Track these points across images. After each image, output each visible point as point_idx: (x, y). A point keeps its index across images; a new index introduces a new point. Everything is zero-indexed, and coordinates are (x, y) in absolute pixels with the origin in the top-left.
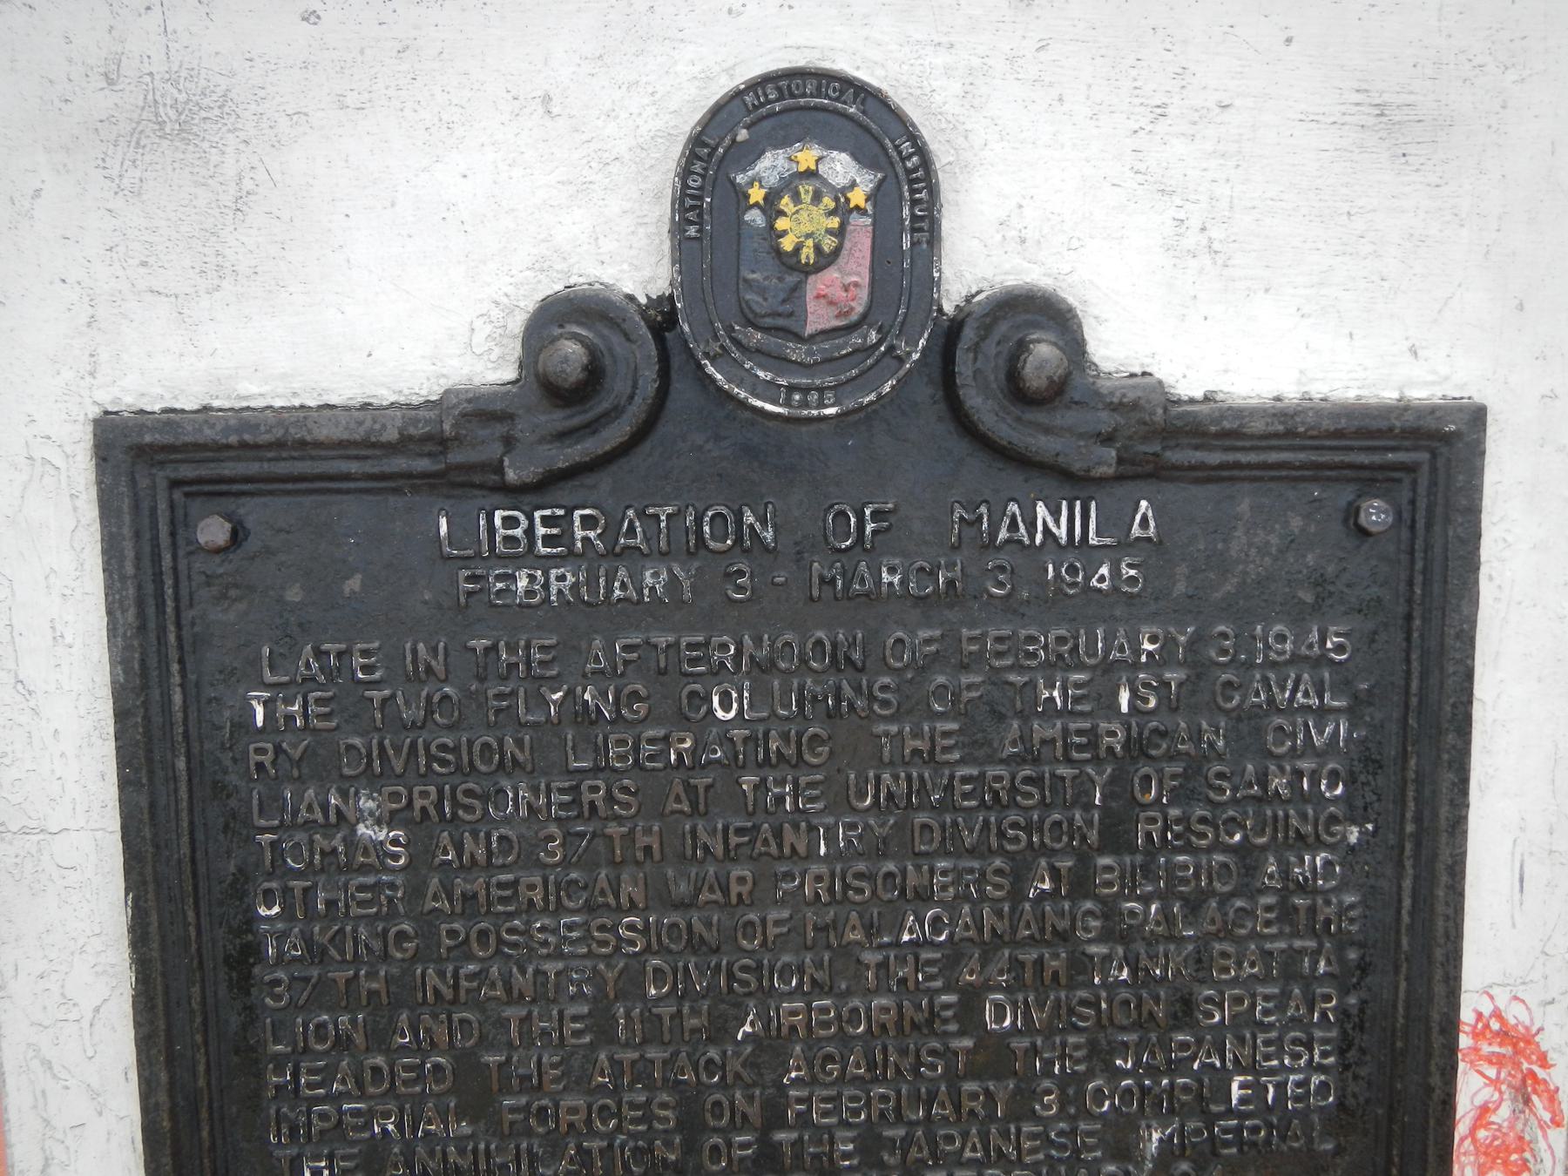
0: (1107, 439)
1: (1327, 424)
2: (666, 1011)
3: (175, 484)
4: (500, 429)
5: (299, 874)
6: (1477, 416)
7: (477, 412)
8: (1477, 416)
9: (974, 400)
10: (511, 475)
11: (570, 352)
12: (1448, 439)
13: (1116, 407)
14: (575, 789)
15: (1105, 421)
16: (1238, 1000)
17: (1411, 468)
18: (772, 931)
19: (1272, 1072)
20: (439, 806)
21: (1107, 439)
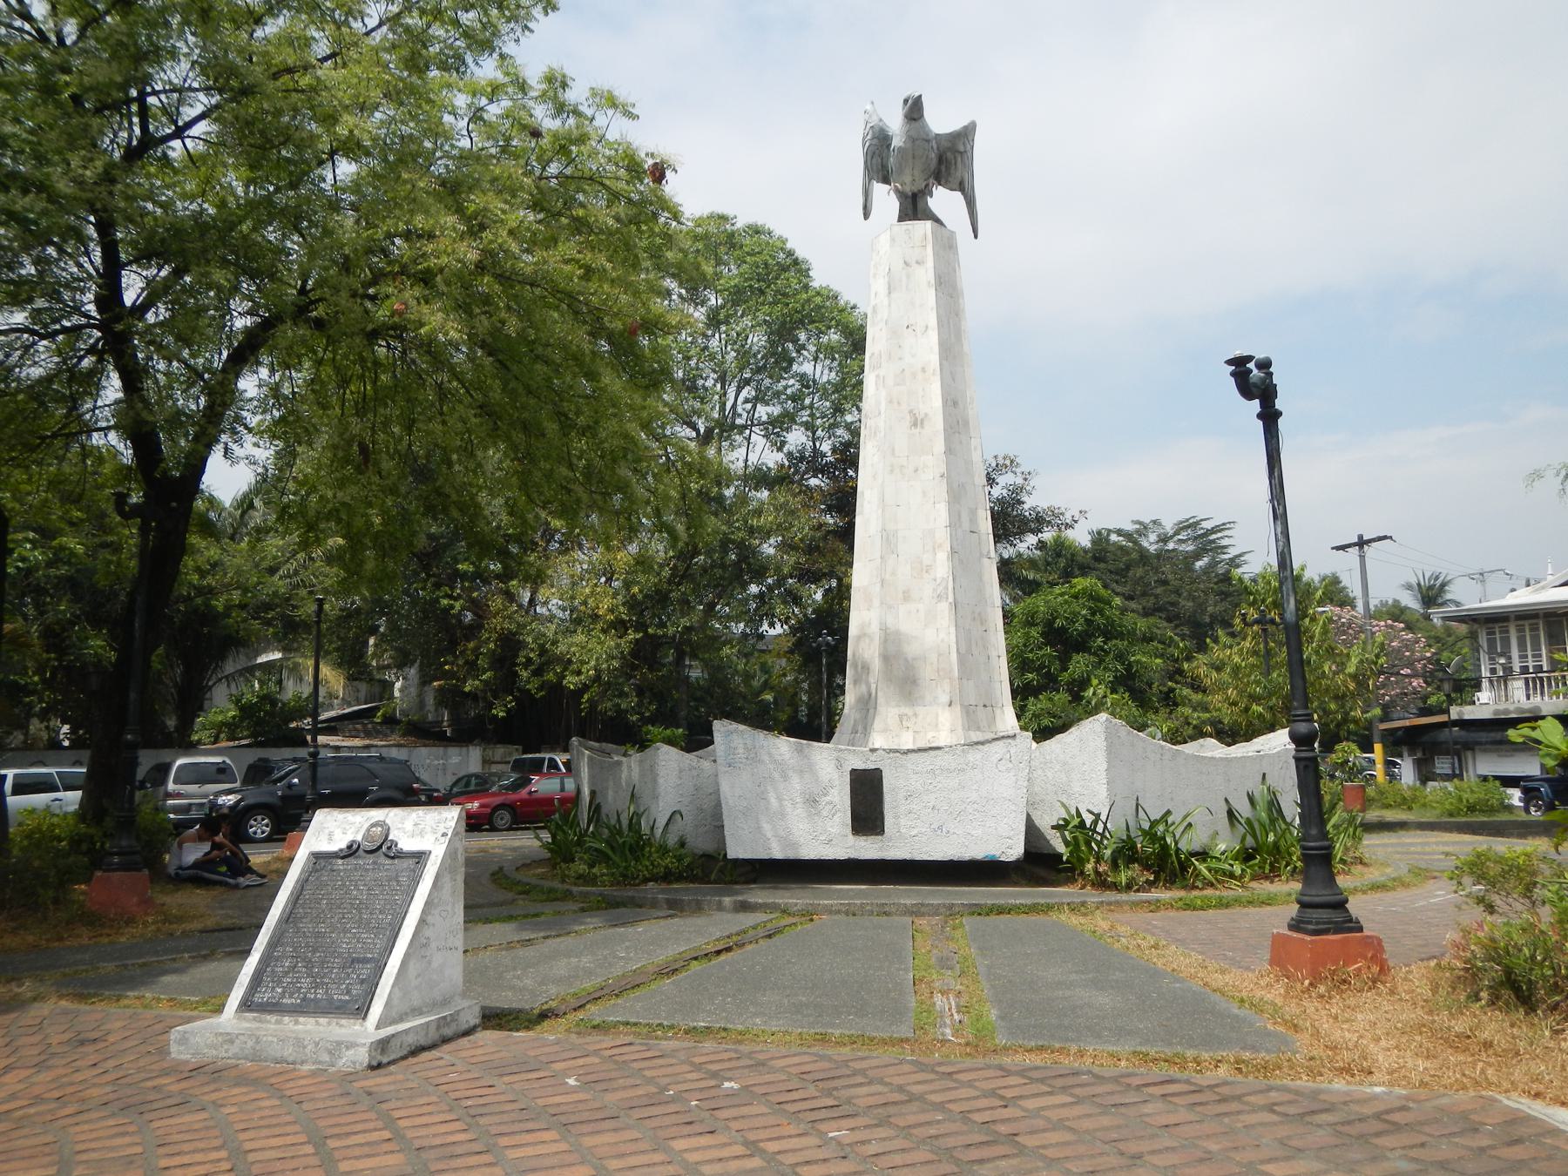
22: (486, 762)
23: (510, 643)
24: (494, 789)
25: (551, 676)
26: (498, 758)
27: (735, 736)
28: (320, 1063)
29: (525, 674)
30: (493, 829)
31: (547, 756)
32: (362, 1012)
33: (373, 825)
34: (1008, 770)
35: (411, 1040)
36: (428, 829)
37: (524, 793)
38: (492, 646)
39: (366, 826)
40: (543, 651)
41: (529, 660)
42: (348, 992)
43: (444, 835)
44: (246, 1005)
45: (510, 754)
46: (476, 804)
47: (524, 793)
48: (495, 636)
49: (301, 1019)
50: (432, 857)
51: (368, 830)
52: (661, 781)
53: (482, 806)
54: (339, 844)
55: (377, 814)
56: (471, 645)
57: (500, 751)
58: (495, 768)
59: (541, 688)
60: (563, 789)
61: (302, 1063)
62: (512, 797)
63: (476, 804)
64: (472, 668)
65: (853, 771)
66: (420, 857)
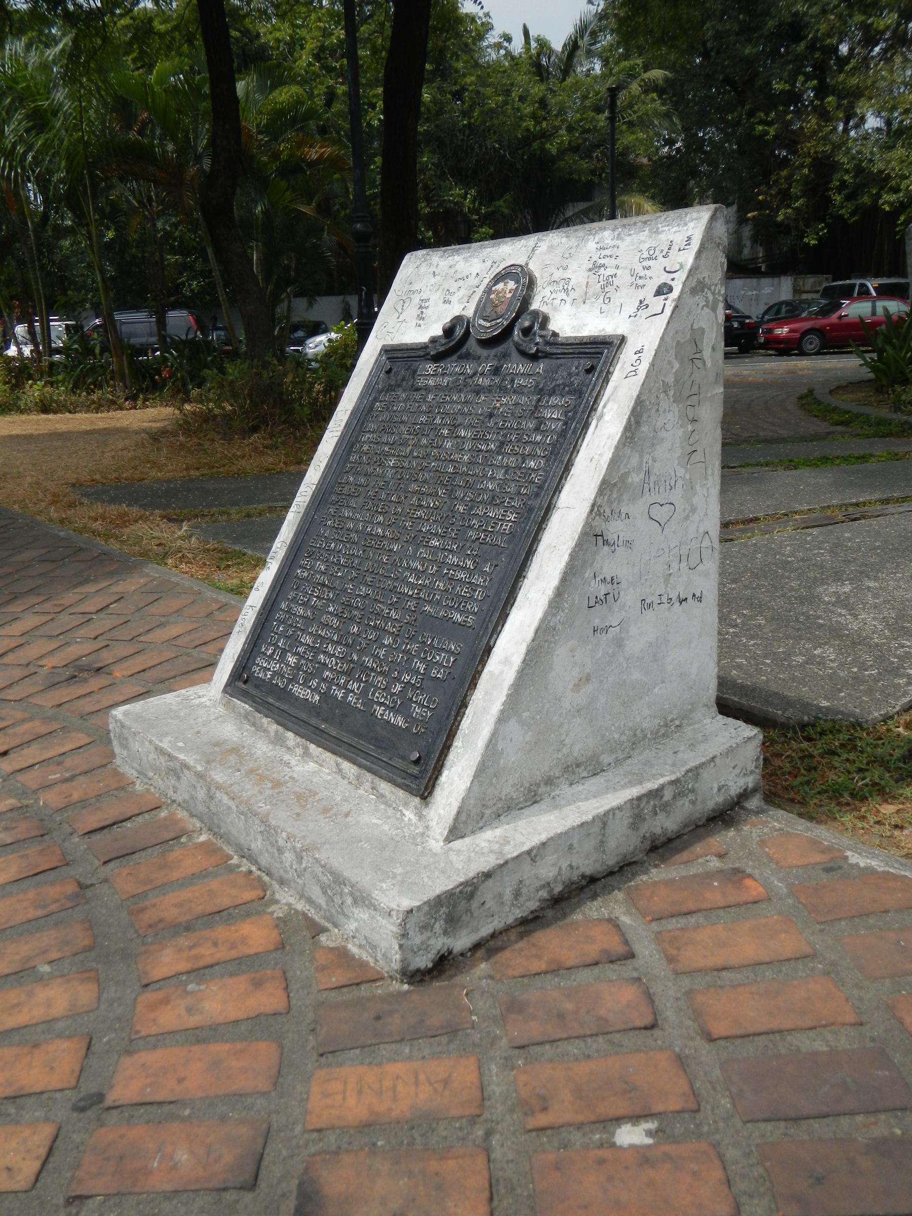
22: (796, 291)
23: (824, 167)
24: (804, 315)
25: (866, 199)
26: (808, 288)
29: (838, 198)
30: (802, 354)
31: (858, 282)
32: (422, 780)
33: (499, 278)
35: (552, 871)
36: (623, 277)
37: (834, 318)
38: (806, 171)
40: (859, 170)
41: (843, 184)
43: (663, 290)
45: (820, 284)
46: (786, 330)
47: (834, 318)
48: (808, 161)
50: (627, 356)
51: (488, 291)
53: (791, 331)
55: (511, 251)
56: (784, 173)
57: (809, 281)
58: (804, 296)
59: (853, 214)
60: (874, 313)
61: (282, 882)
62: (821, 322)
63: (786, 330)
64: (785, 197)
66: (598, 353)
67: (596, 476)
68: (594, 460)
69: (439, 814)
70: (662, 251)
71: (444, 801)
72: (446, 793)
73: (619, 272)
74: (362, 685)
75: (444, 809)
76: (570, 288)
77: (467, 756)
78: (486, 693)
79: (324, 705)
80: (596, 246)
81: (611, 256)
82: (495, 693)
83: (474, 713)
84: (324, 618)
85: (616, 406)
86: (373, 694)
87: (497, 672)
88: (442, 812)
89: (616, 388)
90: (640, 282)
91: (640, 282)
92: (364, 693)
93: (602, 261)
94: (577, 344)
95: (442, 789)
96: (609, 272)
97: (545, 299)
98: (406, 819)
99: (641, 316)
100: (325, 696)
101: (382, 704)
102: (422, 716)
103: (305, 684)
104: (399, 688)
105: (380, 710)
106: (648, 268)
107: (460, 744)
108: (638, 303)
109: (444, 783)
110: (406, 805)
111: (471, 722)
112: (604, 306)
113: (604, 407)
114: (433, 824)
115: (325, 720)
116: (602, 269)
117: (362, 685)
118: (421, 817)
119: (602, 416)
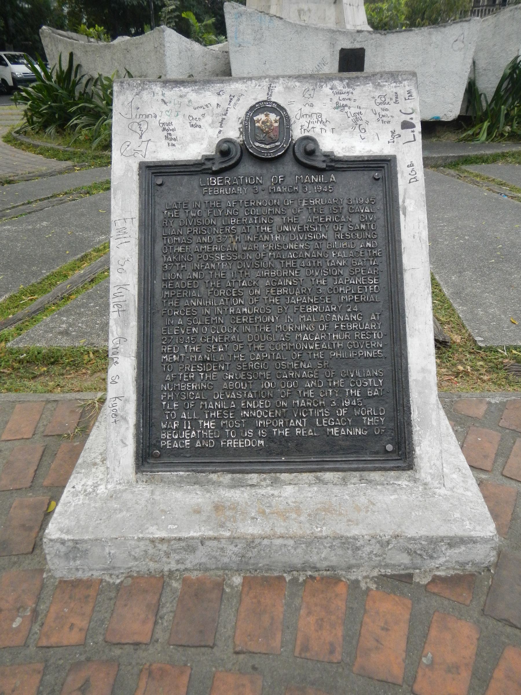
0: (324, 161)
1: (366, 159)
2: (241, 271)
3: (153, 173)
4: (211, 161)
5: (171, 245)
6: (394, 157)
7: (208, 159)
8: (394, 157)
9: (298, 155)
10: (214, 169)
11: (225, 146)
12: (389, 161)
13: (325, 156)
14: (224, 228)
15: (323, 158)
16: (358, 270)
17: (383, 167)
18: (262, 255)
19: (365, 285)
20: (198, 231)
21: (324, 161)
27: (244, 18)
28: (387, 566)
34: (460, 50)
36: (367, 115)
39: (238, 112)
42: (357, 422)
44: (150, 454)
49: (284, 476)
52: (168, 61)
54: (195, 147)
61: (349, 568)
65: (342, 51)
67: (424, 246)
68: (416, 237)
69: (430, 473)
70: (391, 99)
71: (428, 464)
72: (426, 460)
73: (363, 111)
74: (305, 420)
75: (431, 469)
76: (325, 121)
77: (428, 434)
78: (420, 393)
79: (272, 444)
80: (331, 91)
81: (350, 99)
82: (426, 391)
83: (418, 407)
84: (225, 386)
85: (413, 202)
86: (321, 422)
87: (420, 378)
88: (431, 471)
89: (405, 190)
90: (385, 119)
91: (385, 119)
92: (311, 424)
93: (342, 103)
94: (360, 161)
95: (421, 459)
96: (353, 110)
97: (305, 127)
98: (405, 486)
99: (398, 142)
100: (270, 439)
101: (335, 426)
102: (376, 422)
103: (239, 436)
104: (343, 412)
105: (335, 431)
106: (387, 110)
107: (418, 428)
108: (390, 134)
109: (420, 455)
110: (398, 478)
111: (419, 413)
112: (362, 135)
113: (404, 202)
114: (429, 479)
115: (281, 454)
116: (346, 108)
117: (305, 420)
118: (415, 481)
119: (405, 209)
